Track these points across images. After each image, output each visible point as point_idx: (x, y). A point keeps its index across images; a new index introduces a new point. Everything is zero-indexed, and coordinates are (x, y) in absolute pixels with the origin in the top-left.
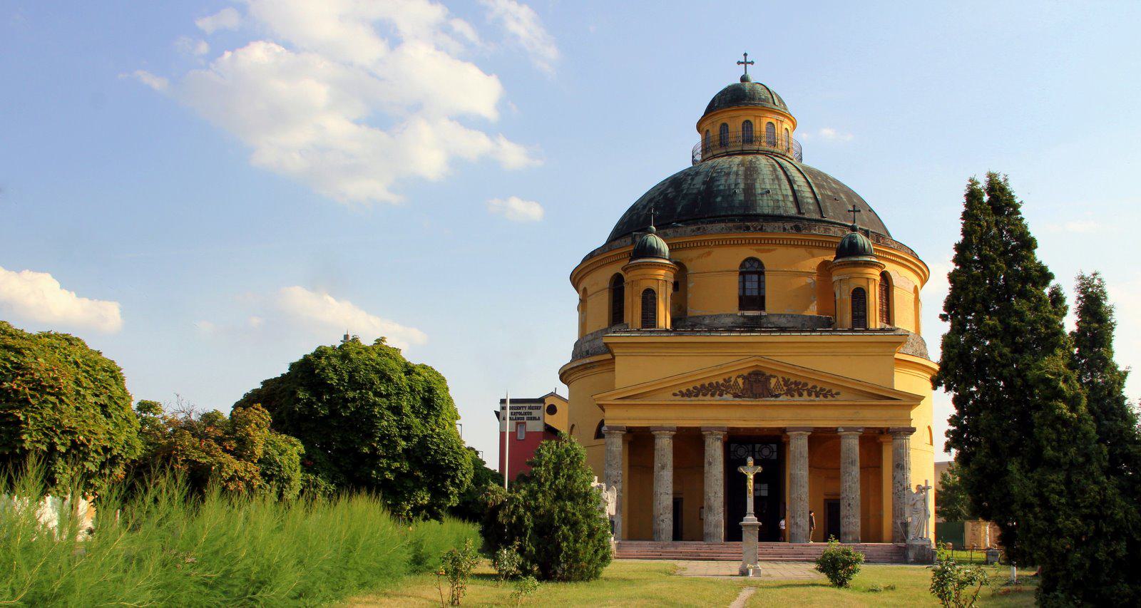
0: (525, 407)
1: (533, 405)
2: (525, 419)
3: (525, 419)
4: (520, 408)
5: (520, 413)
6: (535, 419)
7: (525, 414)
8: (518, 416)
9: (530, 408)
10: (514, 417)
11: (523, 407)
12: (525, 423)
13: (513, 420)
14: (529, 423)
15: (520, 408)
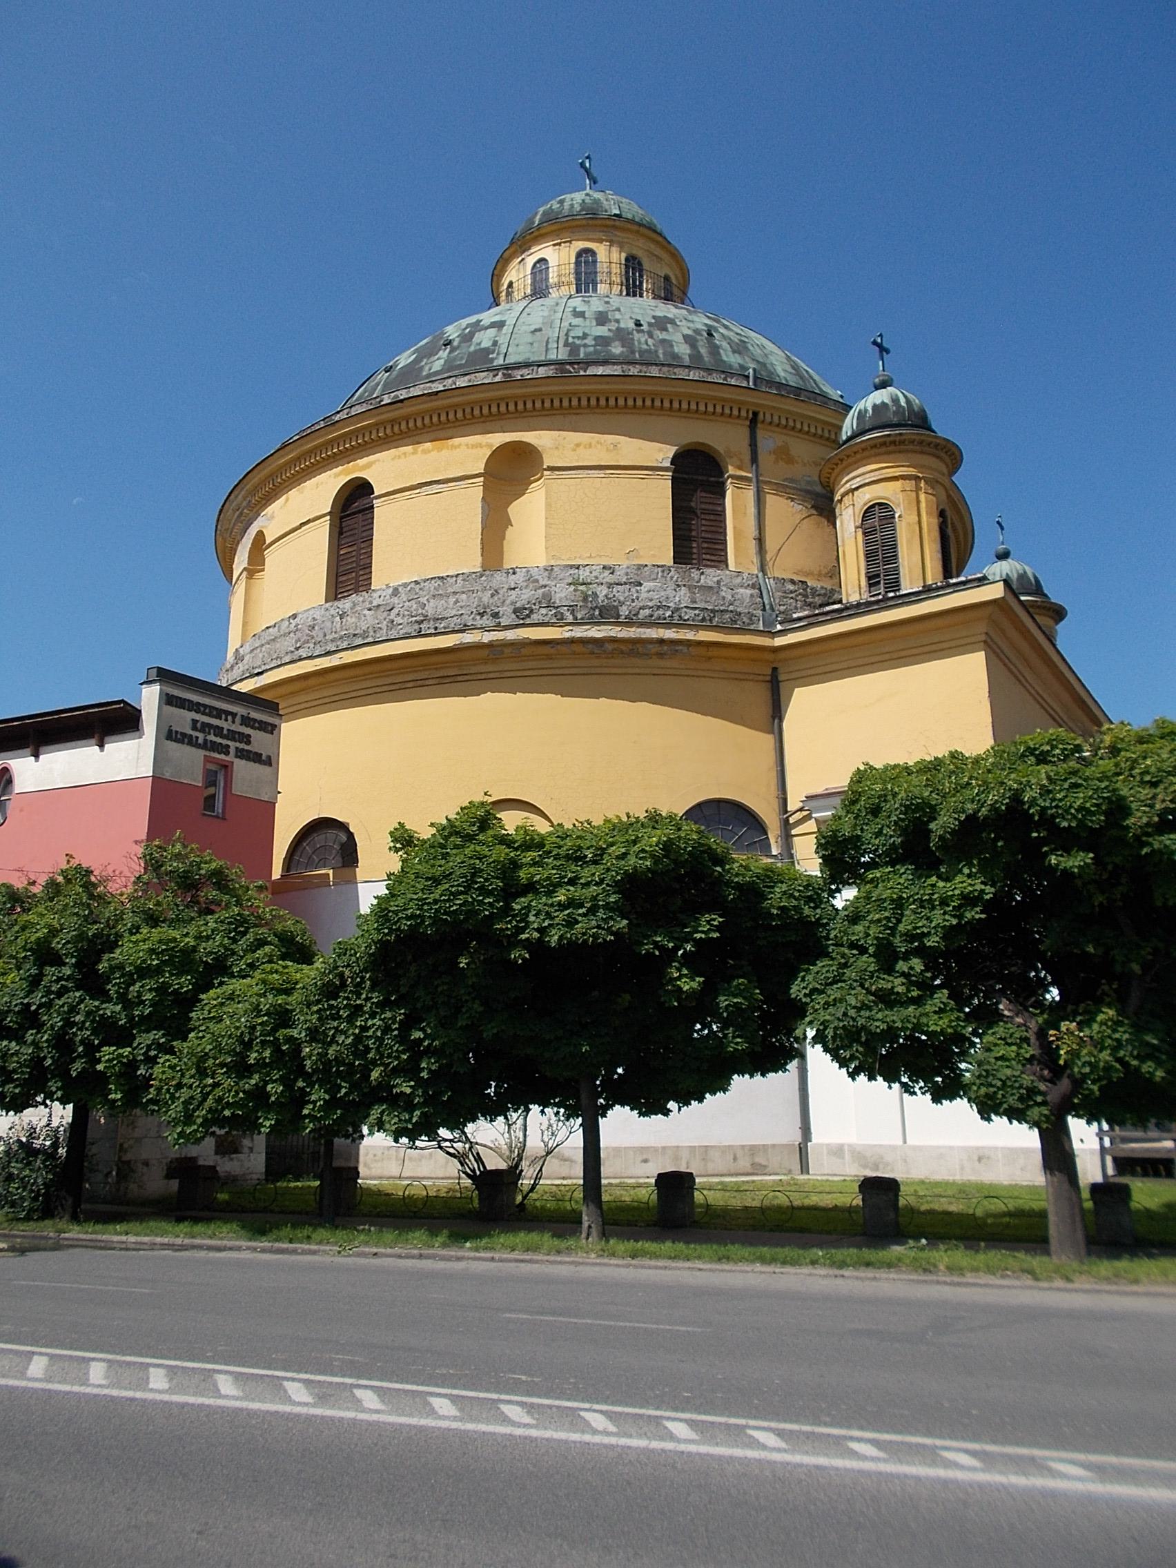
0: (234, 715)
1: (255, 715)
2: (232, 751)
3: (232, 751)
4: (219, 713)
5: (219, 731)
6: (256, 758)
7: (232, 735)
8: (212, 737)
9: (246, 721)
10: (201, 736)
11: (228, 713)
12: (226, 767)
13: (197, 746)
14: (241, 767)
15: (219, 713)
